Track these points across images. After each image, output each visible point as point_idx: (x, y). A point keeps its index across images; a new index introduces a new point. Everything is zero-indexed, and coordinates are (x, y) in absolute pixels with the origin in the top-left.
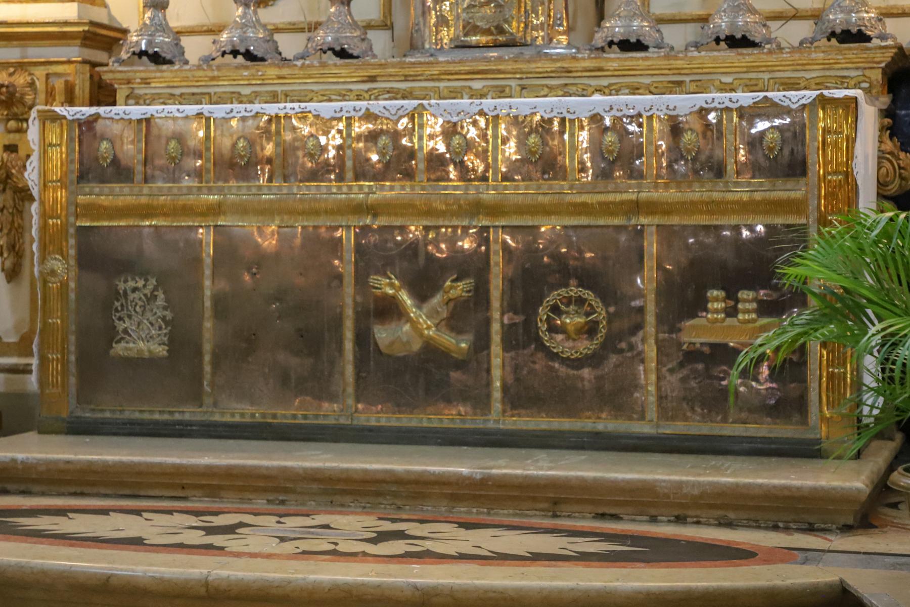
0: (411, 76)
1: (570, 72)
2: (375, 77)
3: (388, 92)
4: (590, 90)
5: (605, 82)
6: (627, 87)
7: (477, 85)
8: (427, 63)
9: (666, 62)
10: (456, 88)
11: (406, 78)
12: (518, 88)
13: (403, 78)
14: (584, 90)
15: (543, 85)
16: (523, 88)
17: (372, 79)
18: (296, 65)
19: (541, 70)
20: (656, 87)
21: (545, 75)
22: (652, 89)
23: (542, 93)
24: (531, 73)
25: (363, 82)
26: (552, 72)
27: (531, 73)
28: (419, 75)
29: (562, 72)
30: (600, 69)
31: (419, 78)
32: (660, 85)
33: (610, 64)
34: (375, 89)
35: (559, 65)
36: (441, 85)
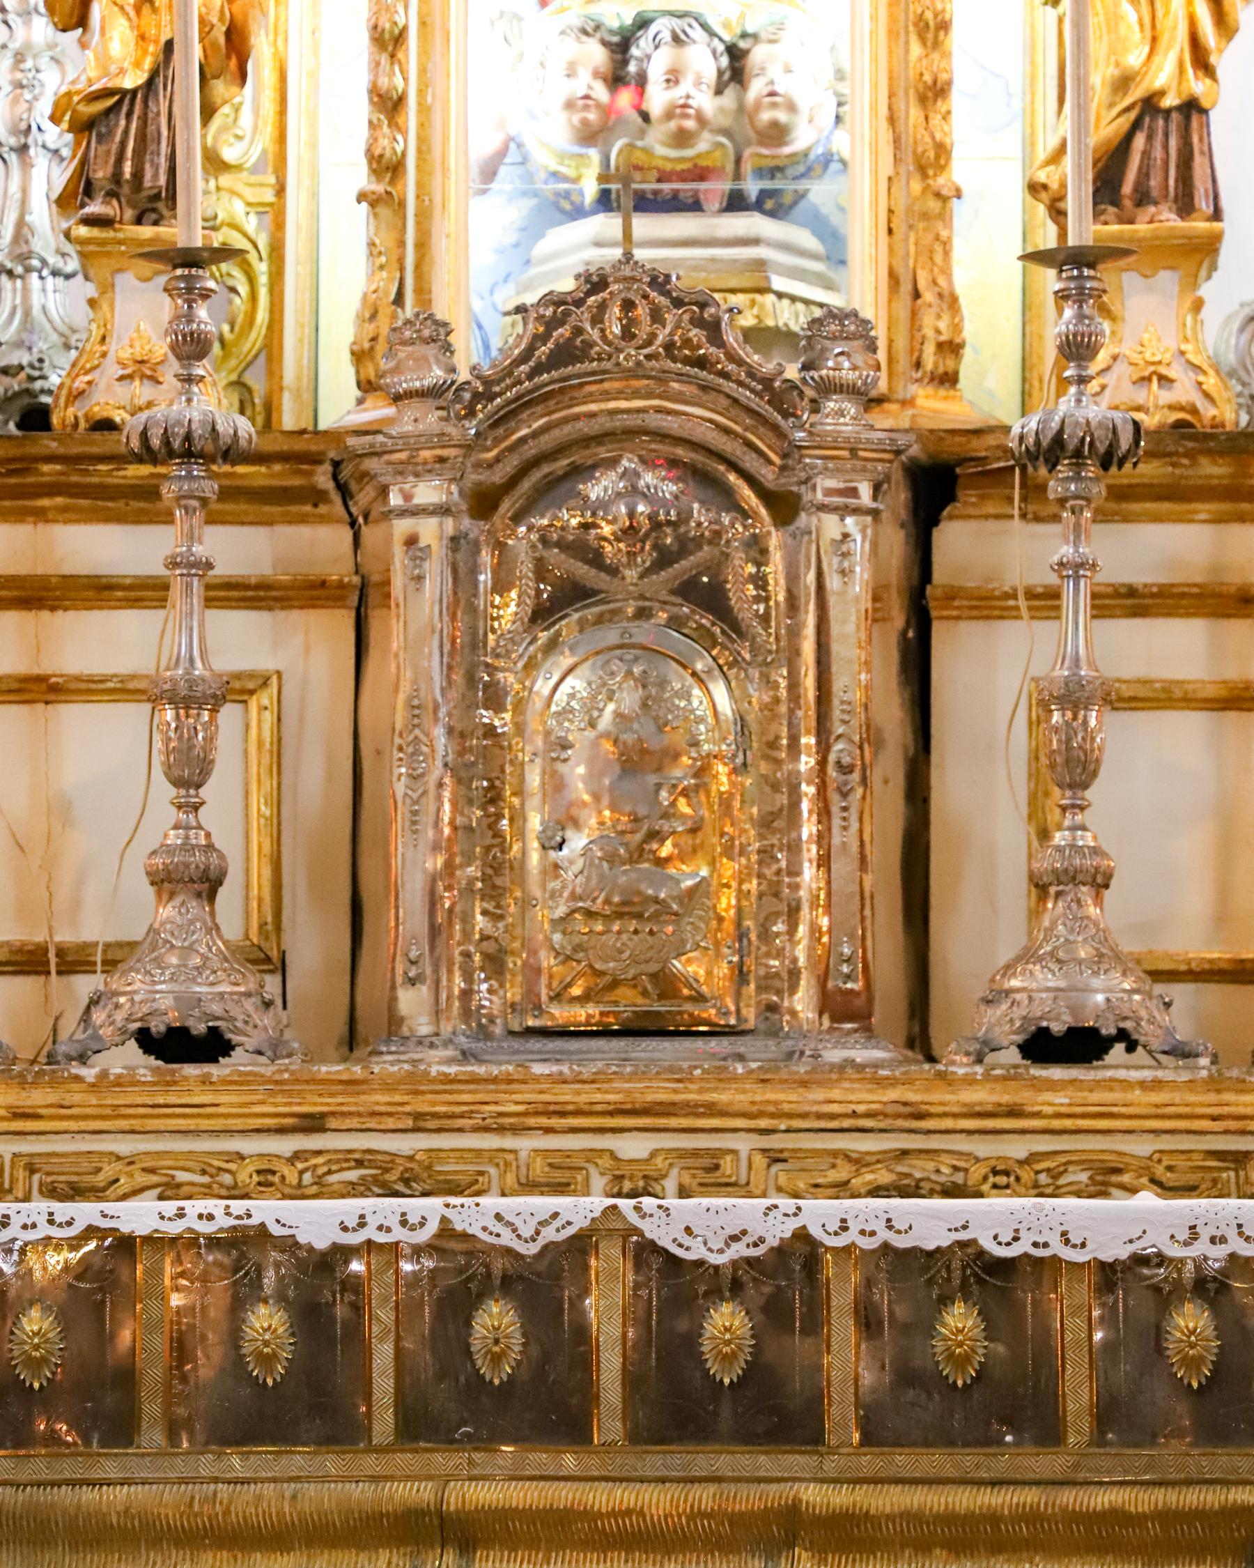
0: (435, 1116)
1: (920, 1116)
2: (323, 1116)
3: (360, 1164)
4: (977, 1172)
5: (1017, 1149)
6: (1085, 1164)
7: (633, 1147)
8: (495, 1080)
9: (1212, 1097)
10: (568, 1154)
11: (420, 1124)
12: (760, 1161)
13: (410, 1123)
14: (956, 1169)
15: (835, 1153)
16: (775, 1158)
17: (313, 1124)
18: (78, 1079)
19: (835, 1108)
20: (1170, 1168)
21: (846, 1123)
22: (1159, 1171)
23: (833, 1176)
24: (804, 1116)
25: (281, 1131)
26: (868, 1115)
27: (804, 1116)
28: (462, 1116)
29: (899, 1116)
30: (1014, 1112)
31: (460, 1123)
32: (1181, 1163)
33: (1047, 1096)
34: (319, 1153)
35: (893, 1094)
36: (525, 1144)
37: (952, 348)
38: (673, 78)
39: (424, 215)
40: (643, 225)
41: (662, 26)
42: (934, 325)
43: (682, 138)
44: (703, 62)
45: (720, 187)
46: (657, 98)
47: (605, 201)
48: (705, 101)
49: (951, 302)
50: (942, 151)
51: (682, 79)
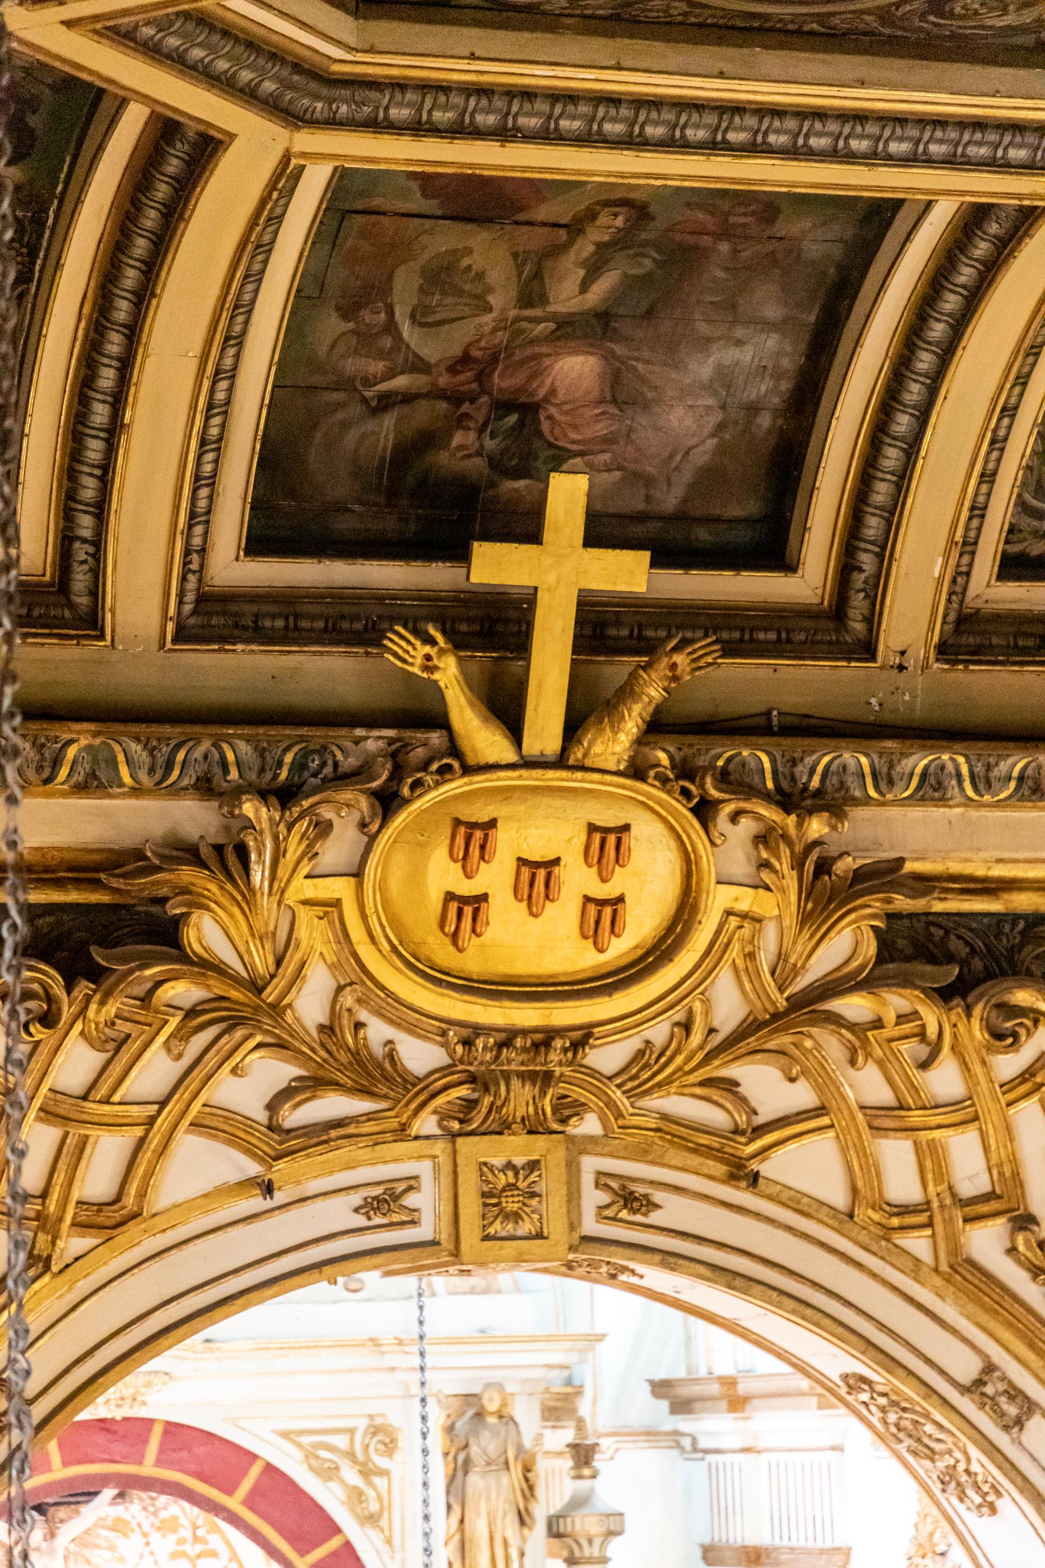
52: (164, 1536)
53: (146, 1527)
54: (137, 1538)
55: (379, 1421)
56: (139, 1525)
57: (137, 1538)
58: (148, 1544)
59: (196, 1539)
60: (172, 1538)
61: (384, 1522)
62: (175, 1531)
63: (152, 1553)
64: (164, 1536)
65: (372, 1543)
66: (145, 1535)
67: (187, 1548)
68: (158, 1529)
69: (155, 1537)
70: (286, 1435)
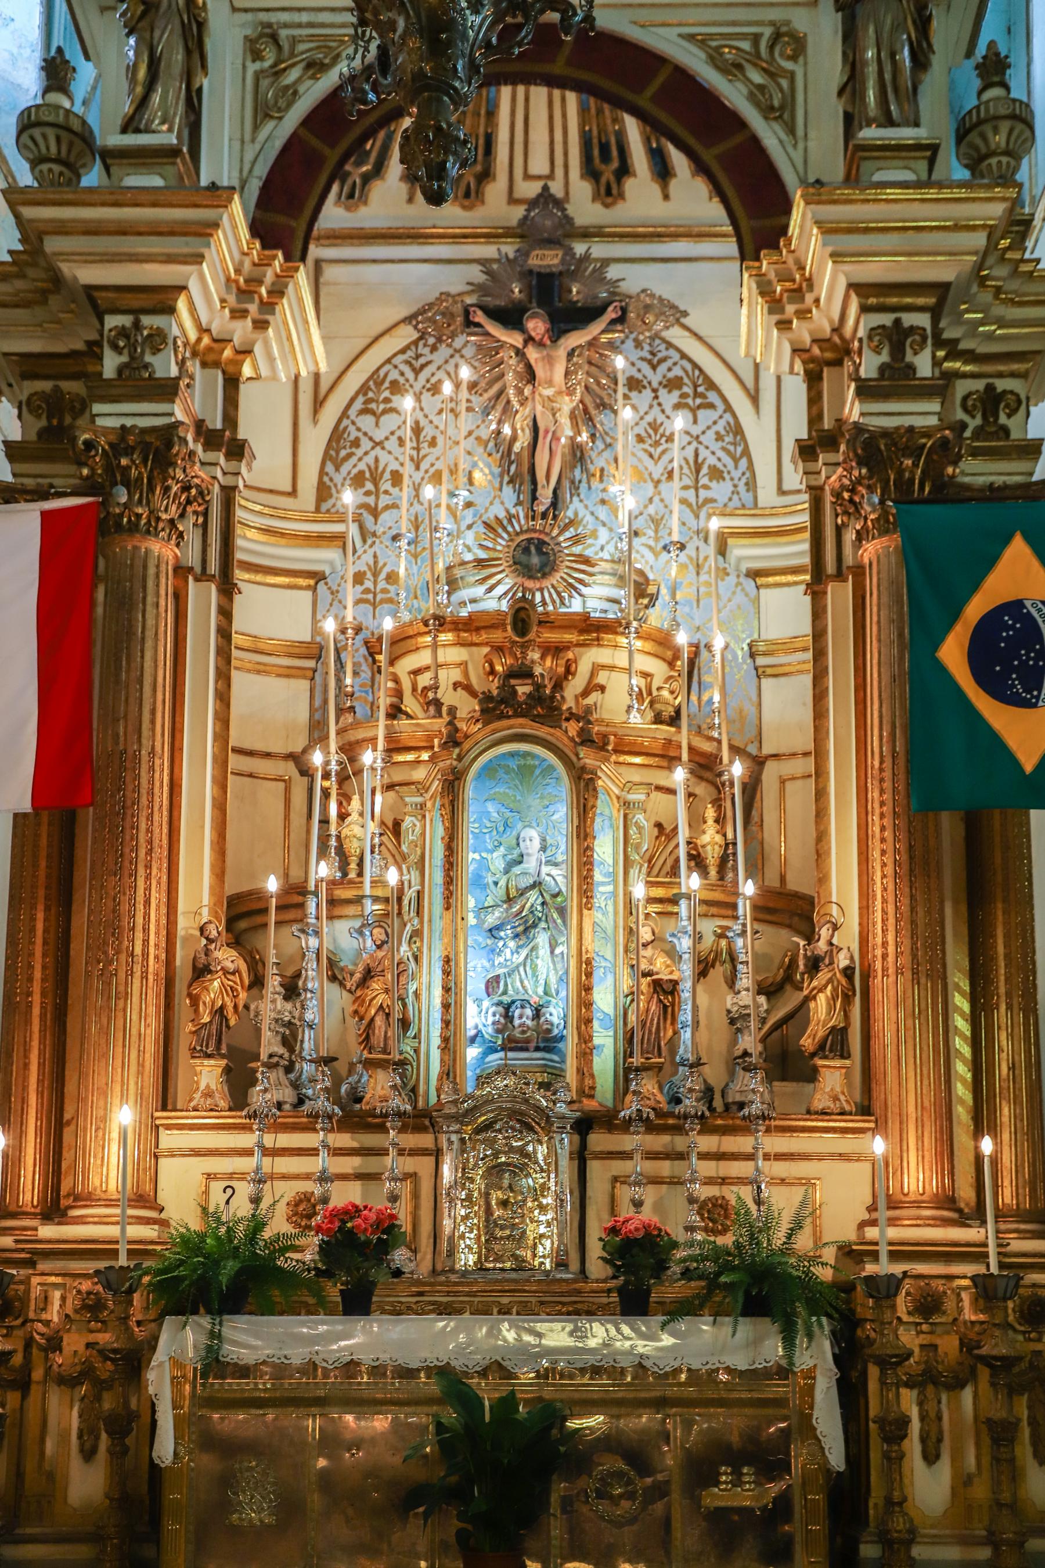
37: (593, 1088)
38: (521, 1017)
39: (455, 1052)
40: (510, 1055)
41: (518, 1003)
42: (588, 1082)
43: (523, 1032)
44: (528, 1012)
45: (533, 1045)
46: (517, 1022)
47: (504, 1048)
48: (529, 1023)
49: (592, 1076)
50: (591, 1037)
51: (523, 1018)
52: (670, 392)
53: (655, 385)
54: (648, 393)
55: (784, 29)
56: (650, 383)
57: (648, 393)
58: (656, 397)
59: (696, 395)
60: (676, 393)
61: (786, 116)
62: (680, 388)
63: (660, 404)
64: (670, 392)
65: (775, 133)
66: (655, 391)
67: (690, 401)
68: (665, 386)
69: (662, 392)
70: (691, 38)
